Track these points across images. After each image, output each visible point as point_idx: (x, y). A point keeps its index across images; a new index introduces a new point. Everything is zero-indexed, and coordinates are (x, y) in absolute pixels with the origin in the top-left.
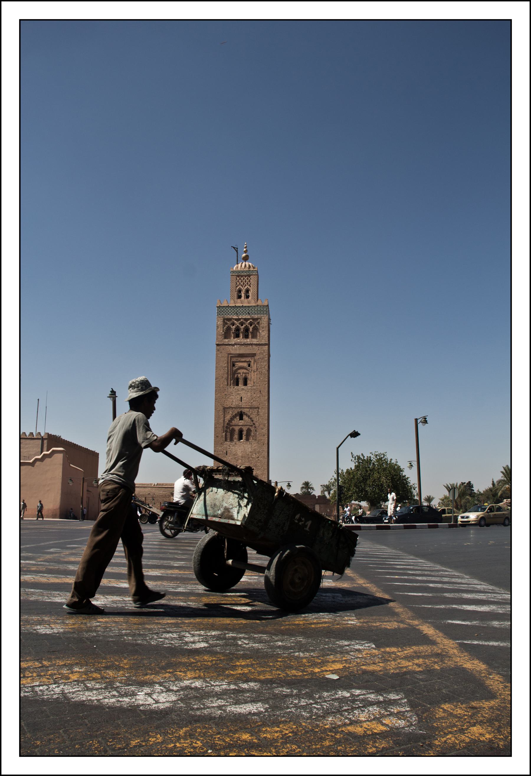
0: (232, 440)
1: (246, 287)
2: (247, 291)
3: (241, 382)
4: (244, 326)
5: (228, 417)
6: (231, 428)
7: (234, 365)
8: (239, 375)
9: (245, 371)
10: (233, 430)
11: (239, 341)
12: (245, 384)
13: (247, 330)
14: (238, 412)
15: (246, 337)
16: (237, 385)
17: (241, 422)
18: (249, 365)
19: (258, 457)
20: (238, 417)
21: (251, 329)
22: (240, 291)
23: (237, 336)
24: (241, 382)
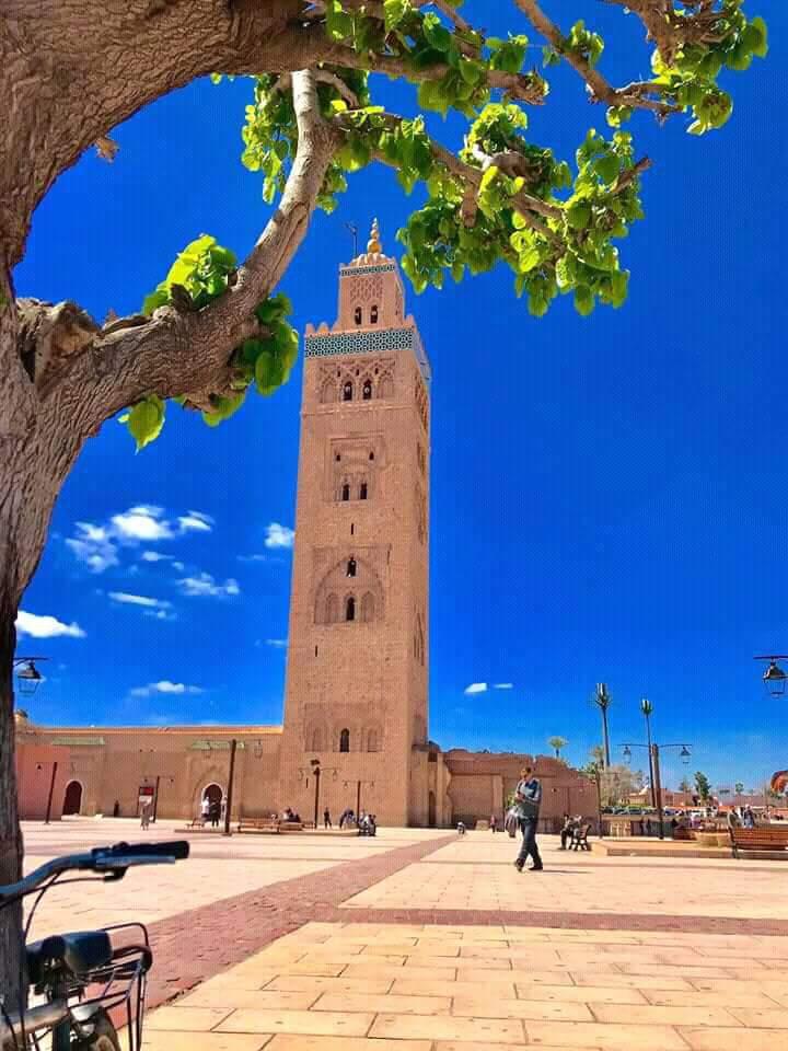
0: (328, 622)
1: (371, 299)
2: (375, 308)
3: (354, 492)
4: (361, 374)
5: (324, 568)
6: (329, 591)
7: (338, 458)
8: (349, 477)
9: (362, 468)
10: (332, 598)
11: (350, 405)
12: (364, 495)
13: (368, 384)
14: (344, 560)
15: (367, 396)
16: (346, 497)
17: (349, 580)
18: (372, 457)
19: (387, 659)
20: (345, 568)
21: (376, 379)
22: (358, 310)
23: (348, 396)
24: (354, 492)
